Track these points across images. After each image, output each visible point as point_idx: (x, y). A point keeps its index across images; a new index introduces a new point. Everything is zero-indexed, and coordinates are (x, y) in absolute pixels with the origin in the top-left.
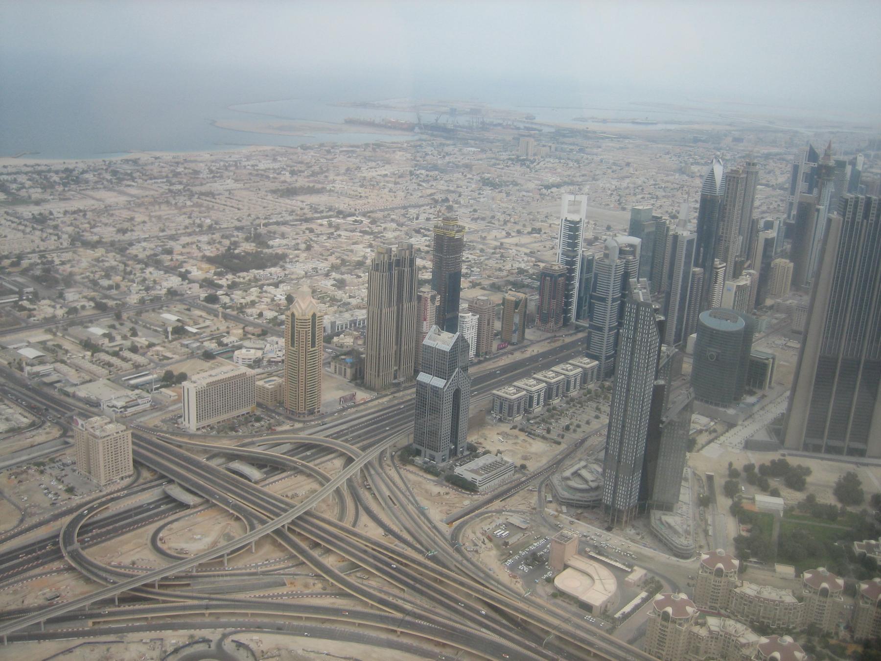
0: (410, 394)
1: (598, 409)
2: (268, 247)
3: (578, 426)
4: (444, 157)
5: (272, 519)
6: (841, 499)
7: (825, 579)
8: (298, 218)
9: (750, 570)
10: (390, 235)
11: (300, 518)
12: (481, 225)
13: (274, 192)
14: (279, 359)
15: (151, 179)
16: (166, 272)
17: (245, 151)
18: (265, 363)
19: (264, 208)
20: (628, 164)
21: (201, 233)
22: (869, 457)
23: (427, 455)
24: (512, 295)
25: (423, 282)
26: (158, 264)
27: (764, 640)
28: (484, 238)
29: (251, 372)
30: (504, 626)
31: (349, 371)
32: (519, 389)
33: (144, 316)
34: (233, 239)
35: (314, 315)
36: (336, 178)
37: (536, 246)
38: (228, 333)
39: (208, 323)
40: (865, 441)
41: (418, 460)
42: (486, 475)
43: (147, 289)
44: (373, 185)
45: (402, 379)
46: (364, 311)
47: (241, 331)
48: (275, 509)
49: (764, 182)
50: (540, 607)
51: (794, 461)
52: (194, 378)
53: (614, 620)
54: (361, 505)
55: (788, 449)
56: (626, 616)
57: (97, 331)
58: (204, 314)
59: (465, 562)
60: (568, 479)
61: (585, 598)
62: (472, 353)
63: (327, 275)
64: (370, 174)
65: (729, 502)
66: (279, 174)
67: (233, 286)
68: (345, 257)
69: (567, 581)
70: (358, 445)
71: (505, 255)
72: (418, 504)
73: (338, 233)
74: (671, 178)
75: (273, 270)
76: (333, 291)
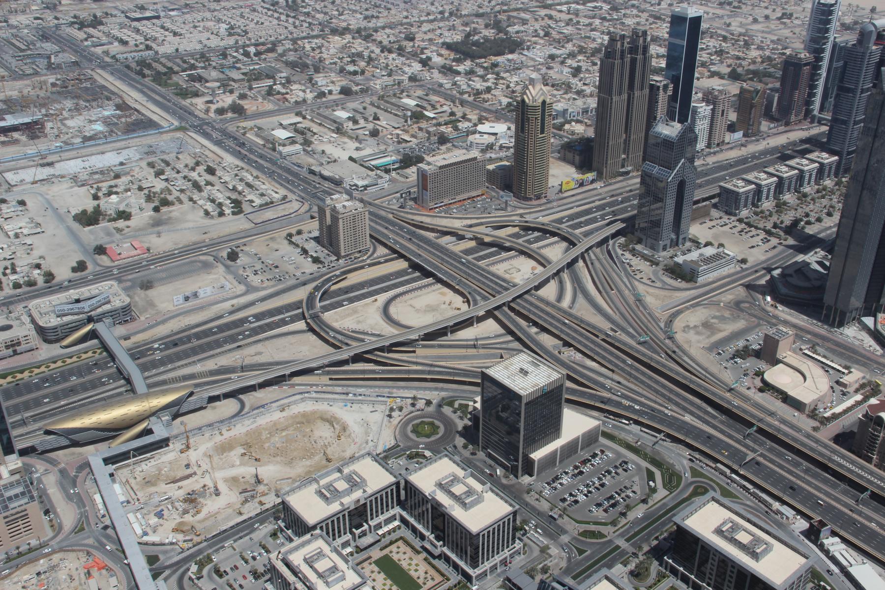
5: (494, 296)
11: (520, 296)
31: (577, 158)
32: (750, 182)
35: (544, 102)
43: (390, 75)
45: (630, 168)
48: (497, 288)
50: (746, 399)
54: (580, 287)
56: (835, 417)
57: (342, 114)
61: (792, 393)
75: (510, 56)
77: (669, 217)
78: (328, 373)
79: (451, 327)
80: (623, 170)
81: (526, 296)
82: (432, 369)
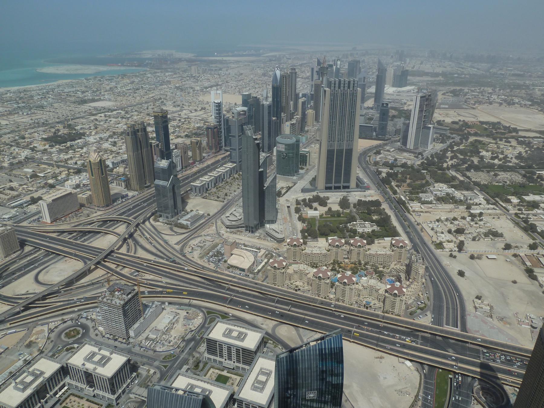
0: (152, 190)
1: (238, 185)
2: (75, 130)
3: (231, 193)
4: (157, 78)
5: (95, 258)
6: (341, 208)
7: (337, 241)
8: (89, 114)
9: (308, 243)
10: (135, 118)
11: (109, 254)
12: (178, 109)
13: (74, 103)
14: (88, 183)
15: (7, 102)
16: (23, 148)
17: (56, 83)
18: (81, 186)
19: (71, 111)
20: (242, 74)
21: (39, 127)
22: (351, 189)
23: (165, 217)
24: (194, 139)
25: (152, 139)
26: (18, 145)
27: (315, 270)
28: (180, 115)
29: (75, 191)
30: (208, 285)
31: (123, 184)
32: (202, 181)
33: (14, 172)
34: (56, 128)
35: (100, 160)
36: (105, 93)
37: (204, 116)
38: (60, 174)
39: (49, 171)
40: (349, 183)
41: (161, 219)
42: (192, 221)
43: (14, 158)
44: (124, 95)
45: (149, 184)
46: (126, 155)
47: (67, 172)
49: (300, 76)
51: (322, 195)
52: (44, 198)
53: (254, 274)
55: (318, 190)
56: (259, 271)
58: (46, 166)
59: (188, 260)
60: (228, 217)
61: (241, 266)
62: (179, 168)
63: (107, 140)
64: (122, 89)
65: (298, 216)
66: (76, 93)
67: (60, 151)
68: (115, 131)
69: (233, 261)
70: (133, 216)
71: (190, 121)
72: (163, 238)
73: (110, 119)
74: (261, 79)
75: (79, 141)
76: (110, 147)
77: (171, 203)
78: (8, 321)
79: (75, 278)
80: (146, 185)
81: (112, 254)
82: (69, 302)
